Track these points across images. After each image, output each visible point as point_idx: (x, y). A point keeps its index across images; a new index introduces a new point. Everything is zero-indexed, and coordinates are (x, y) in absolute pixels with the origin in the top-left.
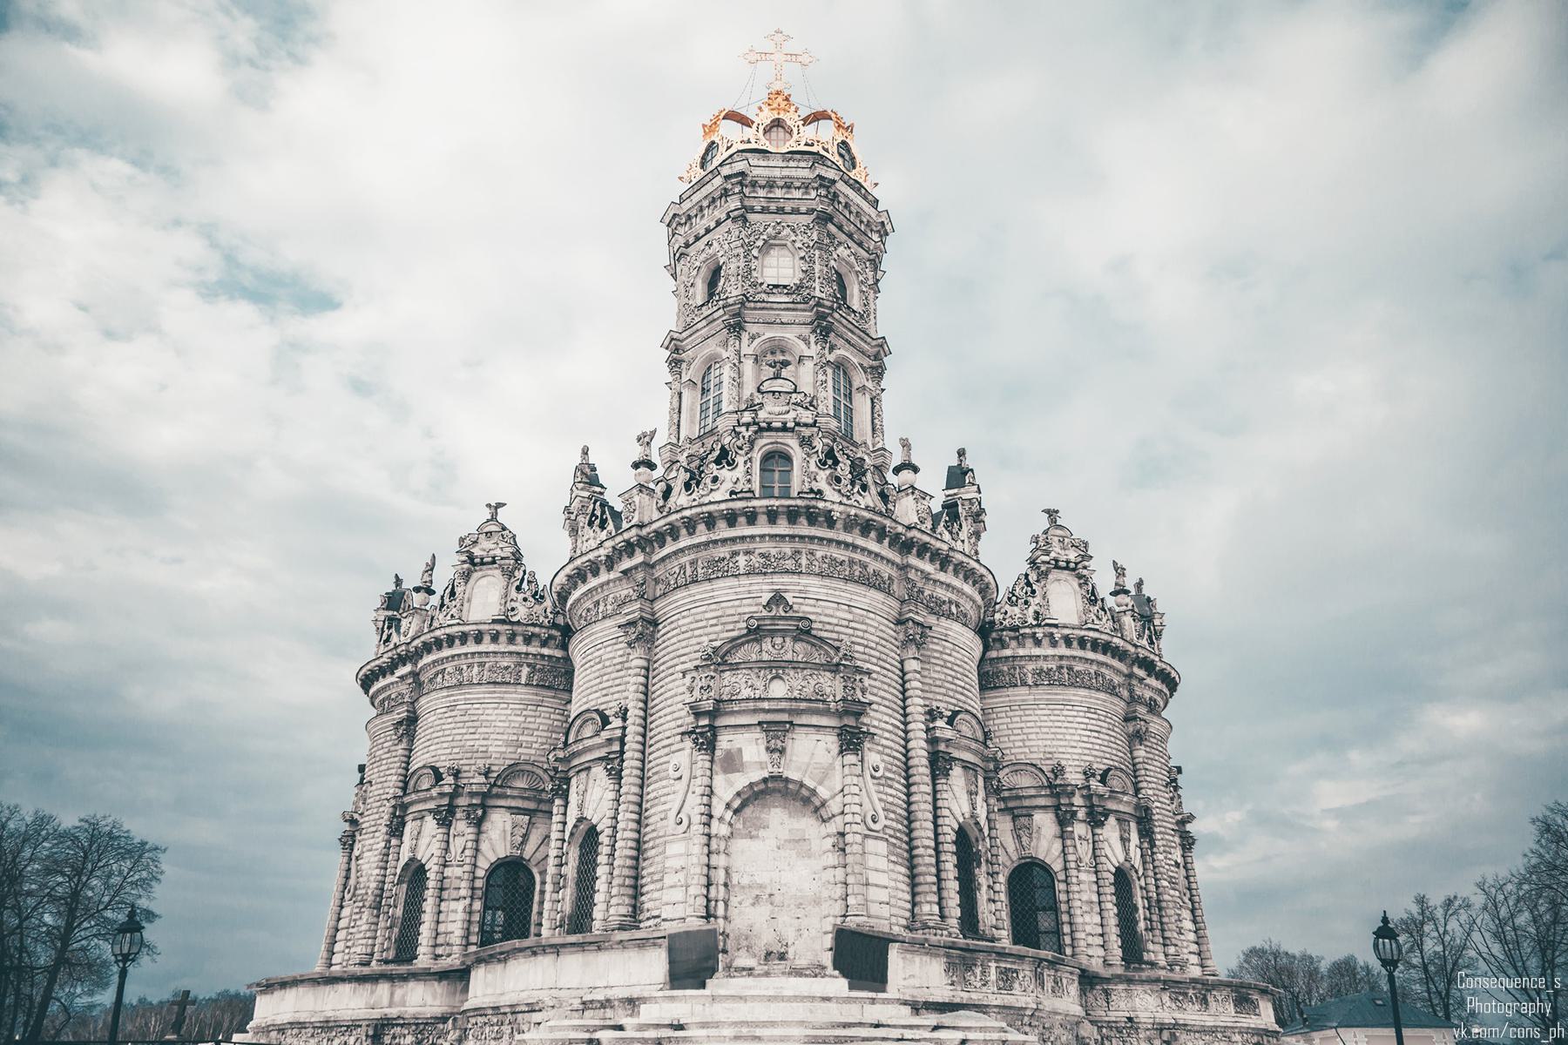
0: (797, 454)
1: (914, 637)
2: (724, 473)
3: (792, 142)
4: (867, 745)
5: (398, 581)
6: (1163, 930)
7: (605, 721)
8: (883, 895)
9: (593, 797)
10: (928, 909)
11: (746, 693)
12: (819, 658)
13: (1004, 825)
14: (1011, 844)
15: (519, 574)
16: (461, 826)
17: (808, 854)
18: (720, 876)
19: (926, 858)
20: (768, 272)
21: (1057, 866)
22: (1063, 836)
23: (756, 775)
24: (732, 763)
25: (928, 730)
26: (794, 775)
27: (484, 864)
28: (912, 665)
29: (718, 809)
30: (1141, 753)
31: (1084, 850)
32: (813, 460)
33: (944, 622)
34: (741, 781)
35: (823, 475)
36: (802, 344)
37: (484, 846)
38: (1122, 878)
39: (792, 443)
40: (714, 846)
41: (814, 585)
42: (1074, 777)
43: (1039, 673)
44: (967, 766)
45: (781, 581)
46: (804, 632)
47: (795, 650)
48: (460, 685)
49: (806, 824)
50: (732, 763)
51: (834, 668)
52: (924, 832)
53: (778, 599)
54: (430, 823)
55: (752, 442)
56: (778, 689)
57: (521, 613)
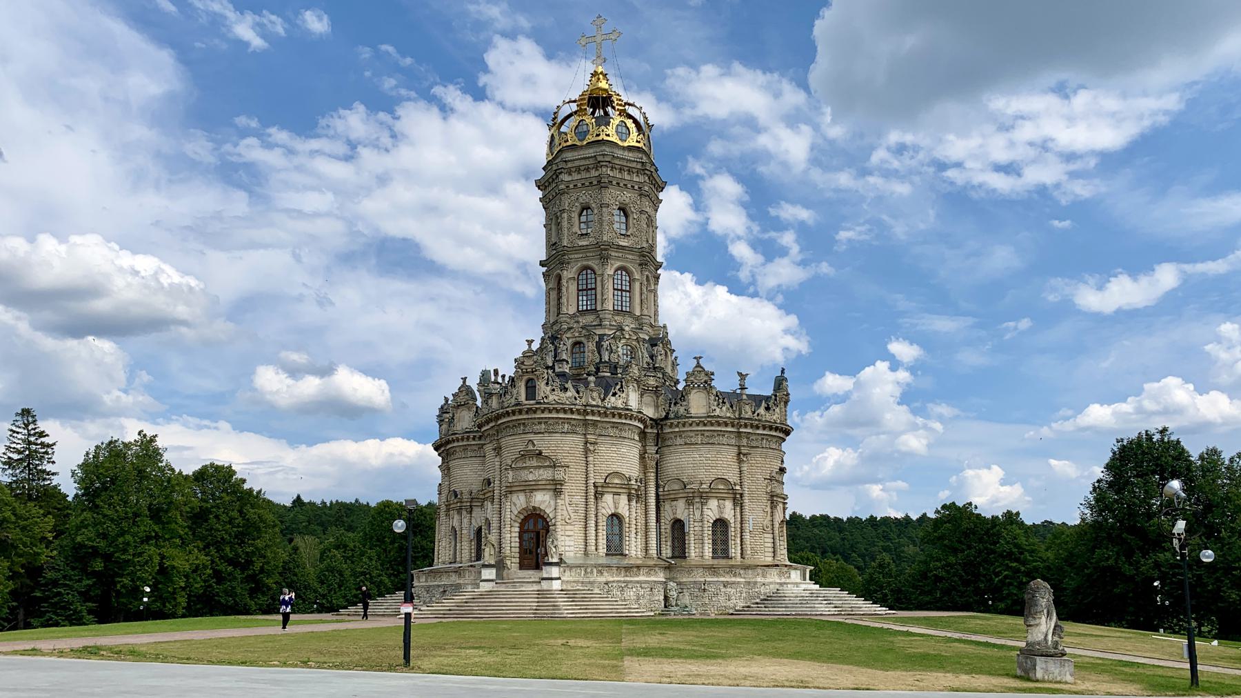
7: (489, 483)
31: (698, 513)
35: (549, 388)
38: (720, 525)
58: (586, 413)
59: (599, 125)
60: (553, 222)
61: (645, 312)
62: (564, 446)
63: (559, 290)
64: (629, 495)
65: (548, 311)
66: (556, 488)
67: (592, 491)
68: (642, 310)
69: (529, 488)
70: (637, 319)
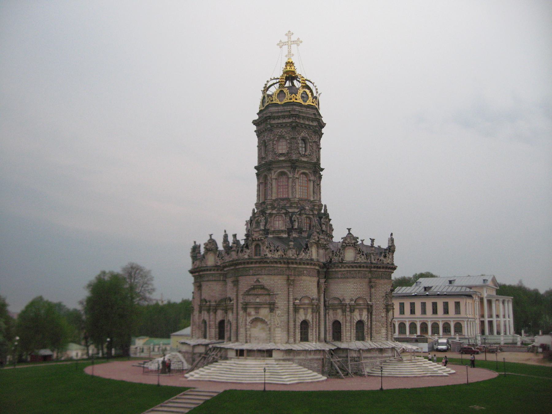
1: (290, 283)
2: (247, 250)
3: (285, 99)
4: (276, 309)
5: (195, 242)
6: (371, 334)
7: (231, 301)
8: (279, 338)
9: (231, 317)
10: (292, 340)
11: (252, 301)
12: (266, 292)
13: (331, 312)
14: (332, 317)
15: (218, 253)
16: (211, 313)
18: (248, 335)
19: (292, 330)
20: (280, 148)
21: (341, 322)
22: (343, 315)
23: (254, 317)
24: (249, 315)
25: (294, 303)
26: (261, 317)
27: (217, 321)
28: (290, 289)
29: (248, 323)
30: (373, 290)
31: (348, 318)
32: (265, 248)
34: (252, 318)
35: (267, 250)
36: (288, 173)
37: (217, 317)
38: (360, 323)
39: (260, 243)
40: (247, 329)
41: (265, 277)
42: (347, 302)
44: (304, 309)
45: (258, 276)
46: (263, 288)
47: (260, 292)
48: (208, 281)
49: (264, 325)
50: (249, 315)
51: (269, 295)
53: (258, 281)
54: (206, 313)
55: (252, 244)
56: (258, 300)
57: (219, 264)
58: (288, 263)
59: (291, 93)
60: (263, 146)
61: (315, 198)
62: (275, 282)
63: (266, 184)
64: (313, 309)
65: (258, 196)
66: (272, 307)
67: (291, 308)
68: (314, 198)
69: (257, 307)
70: (311, 202)
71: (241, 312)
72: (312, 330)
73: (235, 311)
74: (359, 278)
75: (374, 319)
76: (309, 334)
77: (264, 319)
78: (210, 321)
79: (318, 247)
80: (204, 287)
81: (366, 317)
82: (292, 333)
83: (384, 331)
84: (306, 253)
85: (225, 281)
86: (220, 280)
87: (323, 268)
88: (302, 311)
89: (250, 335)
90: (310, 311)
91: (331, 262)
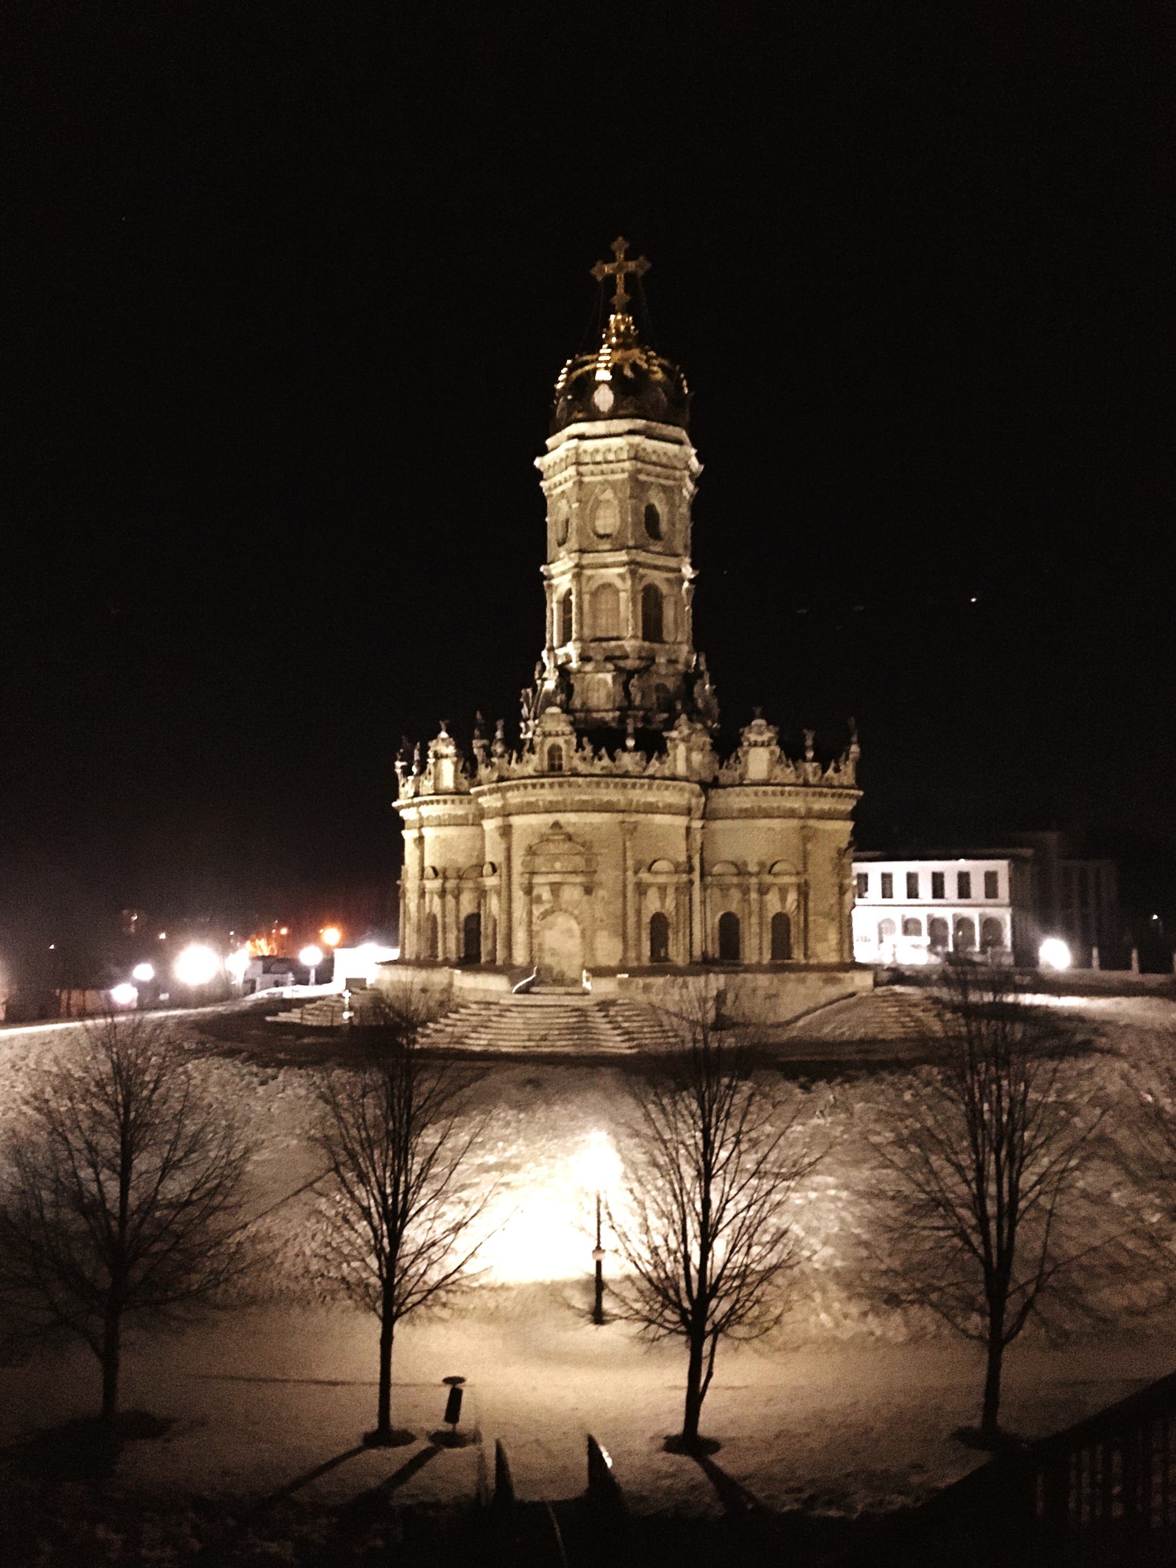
0: (563, 746)
13: (717, 893)
16: (450, 898)
17: (572, 936)
18: (536, 947)
21: (739, 916)
23: (547, 906)
24: (539, 900)
27: (463, 916)
28: (628, 844)
29: (534, 920)
30: (809, 846)
31: (755, 907)
33: (649, 816)
34: (542, 909)
37: (462, 908)
41: (572, 817)
42: (753, 868)
43: (741, 810)
52: (631, 920)
53: (556, 825)
58: (625, 786)
67: (630, 888)
71: (518, 895)
72: (677, 933)
73: (504, 894)
74: (779, 817)
75: (811, 911)
76: (670, 942)
77: (570, 909)
78: (444, 916)
79: (689, 750)
80: (427, 841)
81: (795, 904)
82: (631, 942)
83: (833, 937)
84: (663, 763)
85: (481, 825)
86: (467, 825)
87: (699, 796)
88: (653, 894)
89: (540, 944)
90: (671, 891)
91: (716, 779)
